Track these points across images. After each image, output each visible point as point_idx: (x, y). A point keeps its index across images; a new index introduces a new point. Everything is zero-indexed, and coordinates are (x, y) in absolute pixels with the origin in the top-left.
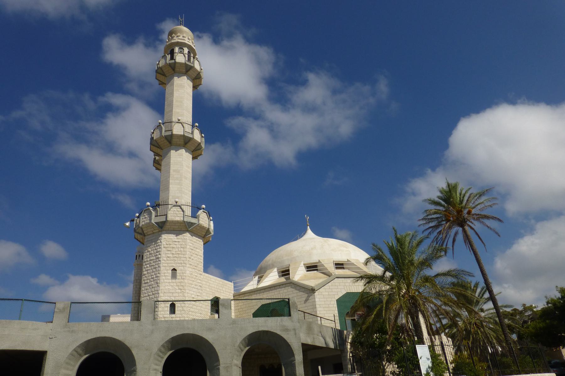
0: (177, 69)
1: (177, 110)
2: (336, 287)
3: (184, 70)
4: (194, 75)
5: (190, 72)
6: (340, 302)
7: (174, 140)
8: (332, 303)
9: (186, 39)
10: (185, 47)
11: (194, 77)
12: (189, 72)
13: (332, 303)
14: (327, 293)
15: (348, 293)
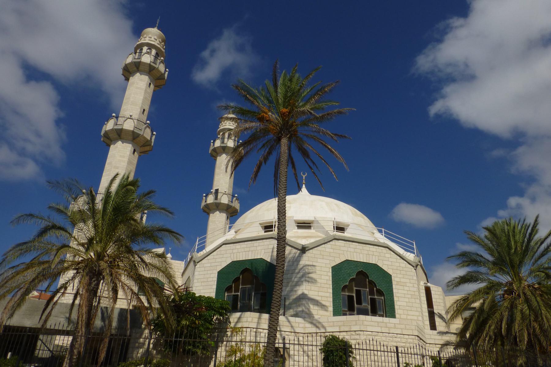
0: (131, 70)
1: (125, 107)
2: (221, 256)
3: (135, 68)
4: (147, 69)
5: (141, 68)
6: (222, 274)
7: (111, 135)
8: (212, 276)
9: (147, 38)
10: (144, 46)
11: (148, 70)
12: (140, 68)
13: (212, 276)
14: (209, 265)
15: (347, 261)
